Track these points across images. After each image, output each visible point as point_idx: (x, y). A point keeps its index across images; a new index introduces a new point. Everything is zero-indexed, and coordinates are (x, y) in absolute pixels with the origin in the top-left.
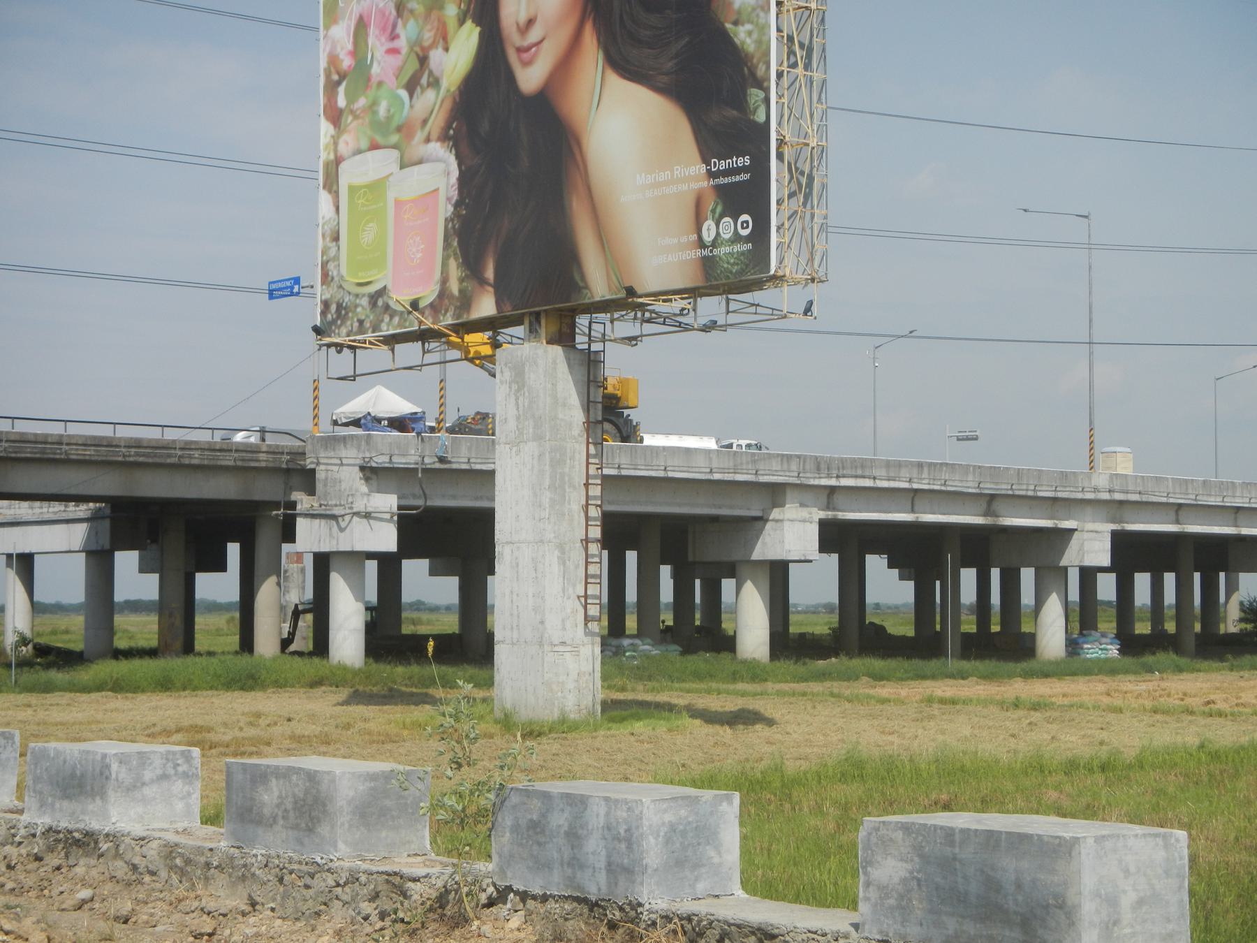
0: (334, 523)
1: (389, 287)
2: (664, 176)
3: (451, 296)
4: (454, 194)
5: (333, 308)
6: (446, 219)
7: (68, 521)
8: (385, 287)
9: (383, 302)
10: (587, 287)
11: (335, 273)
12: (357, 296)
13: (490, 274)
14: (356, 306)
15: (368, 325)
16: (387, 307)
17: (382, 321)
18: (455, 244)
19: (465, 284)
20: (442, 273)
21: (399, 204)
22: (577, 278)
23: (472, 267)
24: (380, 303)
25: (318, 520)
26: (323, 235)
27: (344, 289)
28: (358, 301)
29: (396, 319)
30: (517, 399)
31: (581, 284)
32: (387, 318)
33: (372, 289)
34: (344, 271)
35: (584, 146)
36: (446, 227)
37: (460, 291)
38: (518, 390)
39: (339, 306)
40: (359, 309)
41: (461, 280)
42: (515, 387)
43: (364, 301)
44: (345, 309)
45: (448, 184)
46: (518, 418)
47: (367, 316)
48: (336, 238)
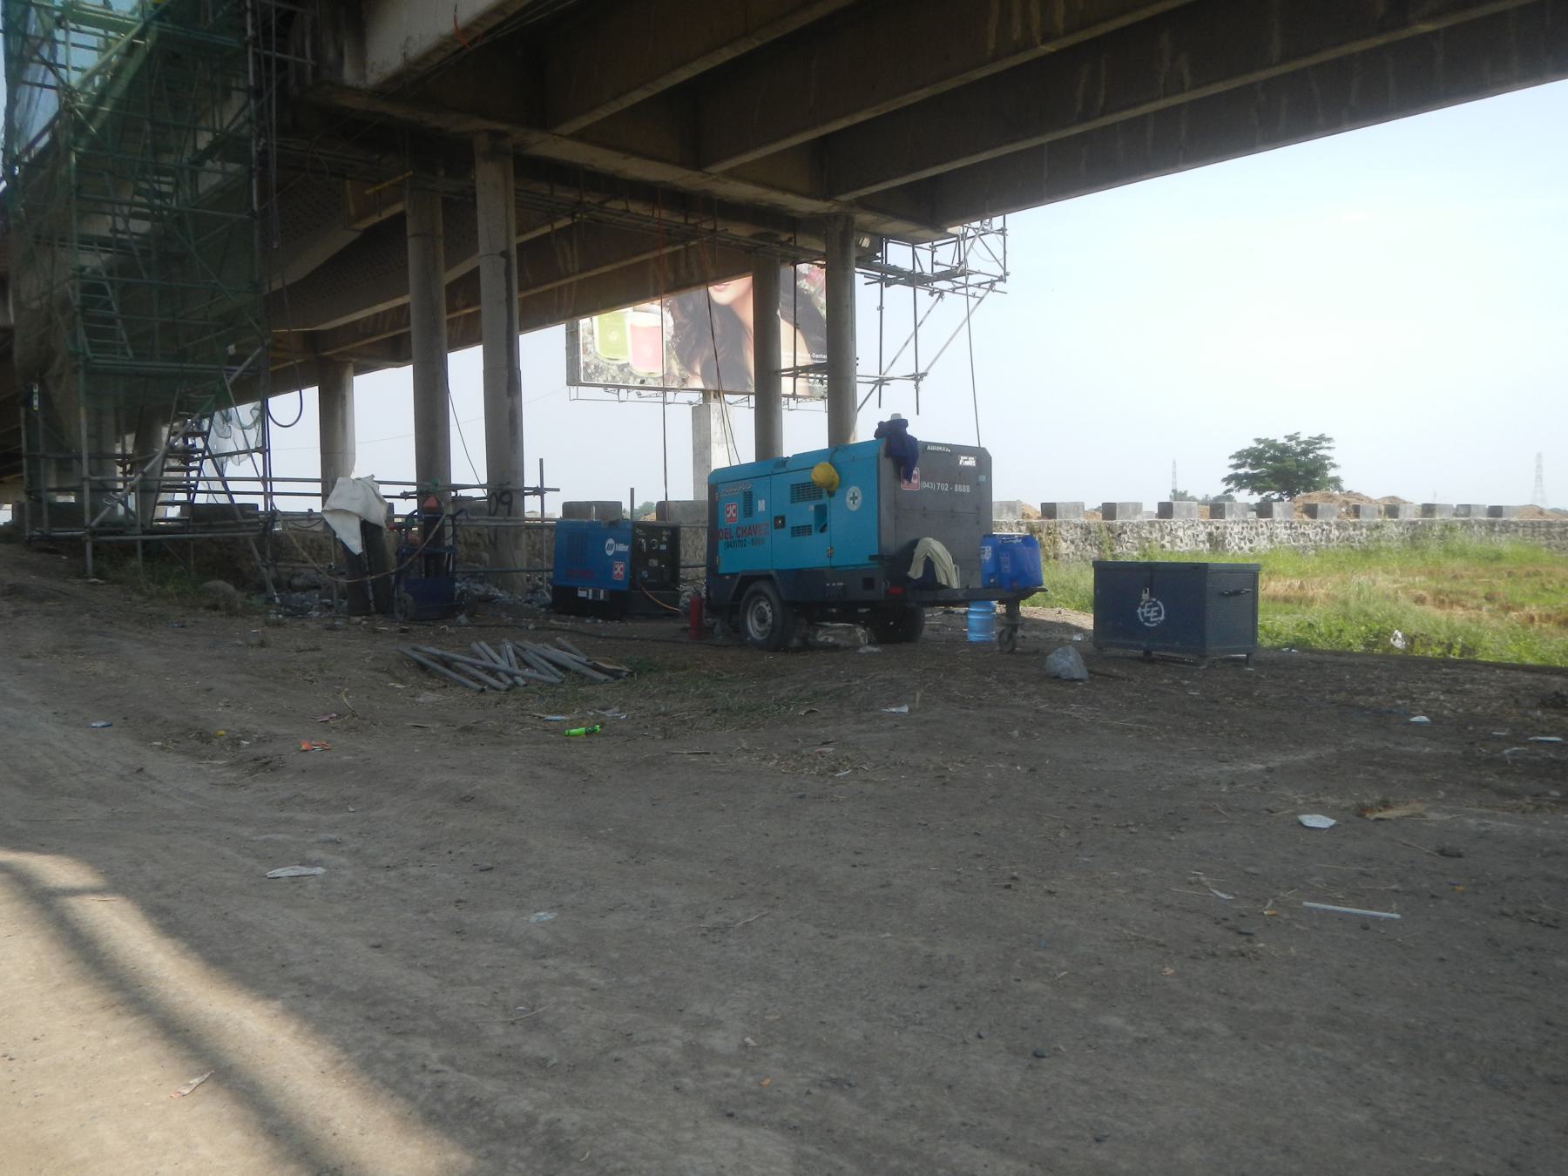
4: (673, 333)
5: (593, 367)
8: (628, 364)
11: (592, 350)
13: (698, 370)
14: (609, 369)
16: (631, 373)
19: (682, 372)
21: (633, 328)
23: (687, 364)
24: (626, 370)
26: (583, 330)
32: (632, 379)
33: (620, 363)
34: (598, 349)
39: (596, 367)
40: (611, 371)
43: (615, 368)
47: (617, 375)
48: (592, 333)
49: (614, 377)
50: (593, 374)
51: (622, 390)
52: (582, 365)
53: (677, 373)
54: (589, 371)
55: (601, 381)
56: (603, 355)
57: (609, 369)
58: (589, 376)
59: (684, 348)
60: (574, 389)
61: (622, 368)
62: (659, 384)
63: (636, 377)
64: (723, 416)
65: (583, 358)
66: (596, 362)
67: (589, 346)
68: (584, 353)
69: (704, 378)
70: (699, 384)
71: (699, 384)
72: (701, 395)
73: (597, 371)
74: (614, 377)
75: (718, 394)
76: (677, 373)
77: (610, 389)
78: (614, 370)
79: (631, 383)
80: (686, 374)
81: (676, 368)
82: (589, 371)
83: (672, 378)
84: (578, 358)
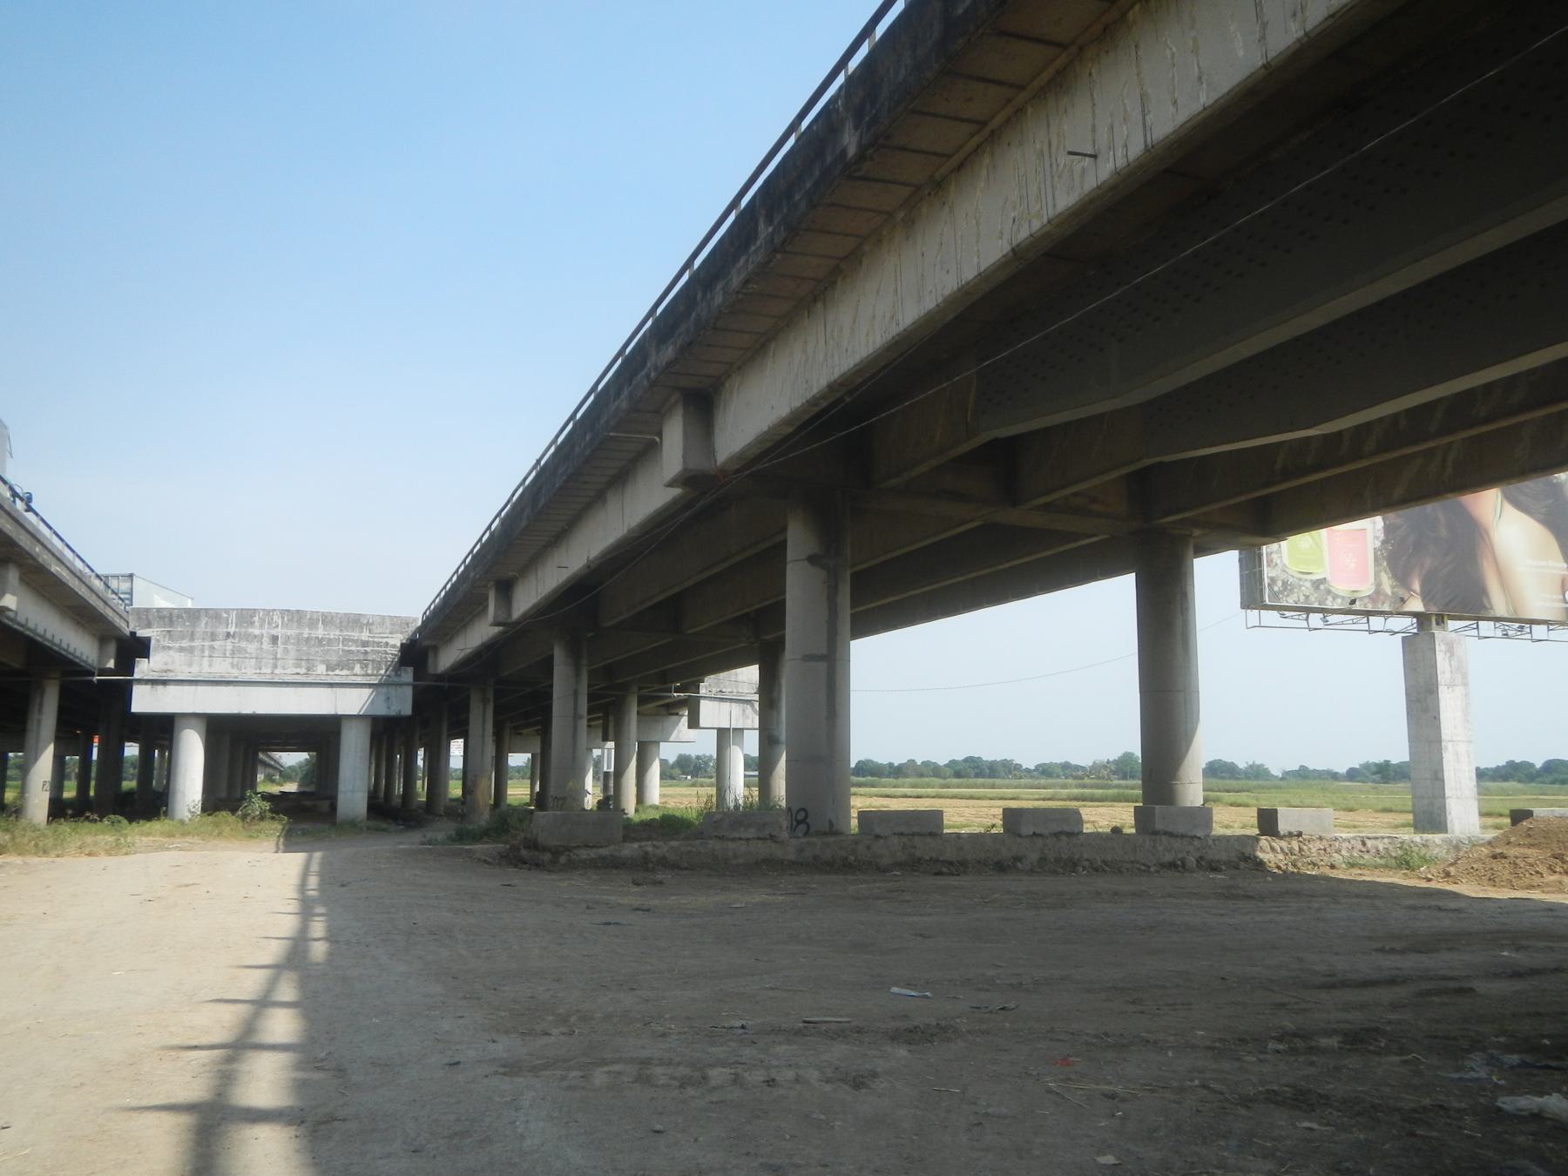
0: (749, 707)
1: (1329, 578)
2: (1544, 563)
3: (1386, 595)
4: (1382, 537)
5: (1280, 583)
6: (1375, 549)
7: (331, 685)
8: (1325, 578)
9: (1325, 588)
10: (1492, 608)
11: (1278, 562)
12: (1300, 579)
13: (1417, 586)
14: (1300, 586)
15: (1313, 600)
16: (1329, 592)
17: (1326, 599)
18: (1385, 564)
19: (1396, 590)
20: (1375, 579)
22: (1485, 602)
23: (1402, 579)
24: (1322, 587)
25: (728, 704)
27: (1287, 573)
28: (1301, 583)
29: (1339, 601)
30: (1450, 661)
31: (1488, 606)
32: (1330, 598)
34: (1286, 561)
35: (1492, 535)
36: (1375, 553)
37: (1392, 592)
38: (1450, 657)
39: (1285, 583)
41: (1393, 587)
42: (1448, 655)
43: (1308, 584)
44: (1290, 585)
45: (1374, 529)
46: (1452, 672)
49: (1307, 597)
50: (1280, 592)
51: (1311, 615)
52: (1266, 581)
53: (1389, 591)
54: (1276, 589)
55: (1290, 602)
56: (1293, 568)
57: (1300, 586)
58: (1275, 595)
59: (1397, 559)
60: (1253, 614)
61: (1317, 584)
62: (1365, 605)
63: (1335, 597)
64: (1450, 651)
65: (1267, 573)
66: (1284, 576)
67: (1274, 556)
68: (1268, 566)
69: (1426, 596)
70: (1416, 605)
71: (1416, 605)
72: (1415, 620)
73: (1285, 589)
74: (1307, 597)
75: (1441, 620)
76: (1389, 591)
77: (1287, 614)
78: (1307, 587)
79: (1329, 604)
80: (1401, 592)
81: (1387, 584)
82: (1276, 589)
83: (1382, 597)
84: (1261, 573)
